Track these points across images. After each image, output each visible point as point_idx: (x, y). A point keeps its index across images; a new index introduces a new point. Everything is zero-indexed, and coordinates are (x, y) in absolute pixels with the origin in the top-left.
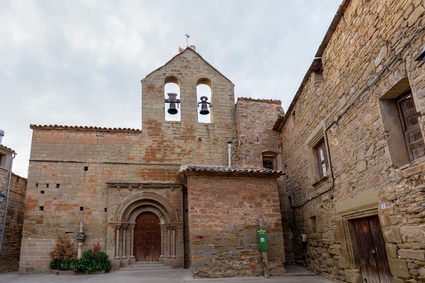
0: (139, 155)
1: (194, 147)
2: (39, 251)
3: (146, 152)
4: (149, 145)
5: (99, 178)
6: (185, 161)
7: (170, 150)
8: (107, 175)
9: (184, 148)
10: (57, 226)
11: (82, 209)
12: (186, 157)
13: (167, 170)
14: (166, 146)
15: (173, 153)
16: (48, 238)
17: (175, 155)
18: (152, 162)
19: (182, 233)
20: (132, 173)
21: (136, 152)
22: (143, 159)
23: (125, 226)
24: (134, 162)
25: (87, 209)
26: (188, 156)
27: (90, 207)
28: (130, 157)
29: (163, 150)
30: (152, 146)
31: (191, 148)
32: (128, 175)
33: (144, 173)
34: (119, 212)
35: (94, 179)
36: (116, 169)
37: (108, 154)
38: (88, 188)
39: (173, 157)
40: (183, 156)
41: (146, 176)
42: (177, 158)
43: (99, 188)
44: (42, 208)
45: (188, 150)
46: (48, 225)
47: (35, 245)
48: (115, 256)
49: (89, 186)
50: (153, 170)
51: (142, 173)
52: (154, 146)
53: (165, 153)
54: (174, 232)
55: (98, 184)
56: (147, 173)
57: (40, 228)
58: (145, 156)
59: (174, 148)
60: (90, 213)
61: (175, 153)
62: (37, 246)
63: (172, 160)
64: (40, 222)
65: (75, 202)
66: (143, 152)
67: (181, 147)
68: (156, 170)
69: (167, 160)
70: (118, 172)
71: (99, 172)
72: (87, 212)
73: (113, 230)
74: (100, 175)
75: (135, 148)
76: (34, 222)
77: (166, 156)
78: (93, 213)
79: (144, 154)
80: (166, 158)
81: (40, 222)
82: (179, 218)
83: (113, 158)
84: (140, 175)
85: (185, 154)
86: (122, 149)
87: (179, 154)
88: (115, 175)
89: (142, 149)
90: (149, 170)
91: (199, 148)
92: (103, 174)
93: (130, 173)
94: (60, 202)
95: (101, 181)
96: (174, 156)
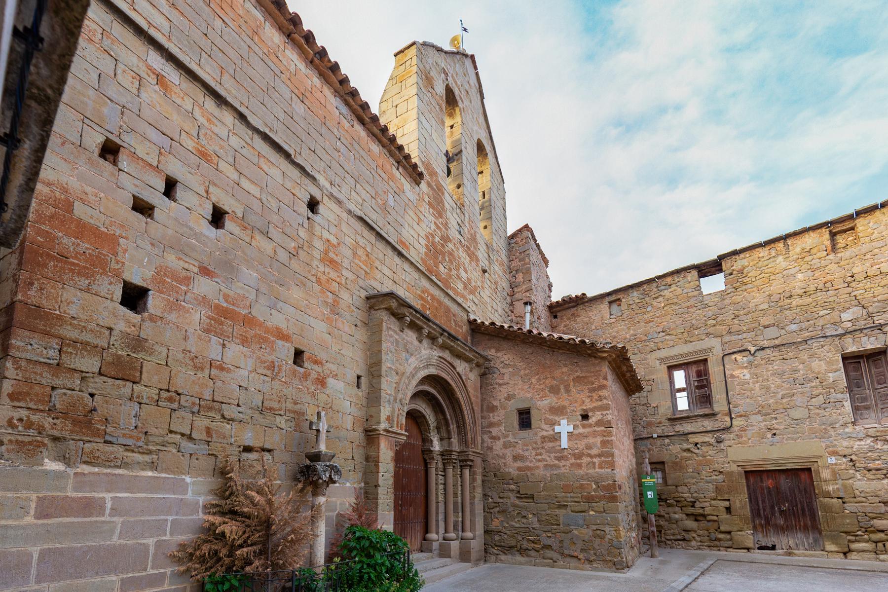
2: (115, 540)
10: (210, 409)
11: (298, 355)
16: (167, 470)
25: (317, 362)
27: (322, 356)
35: (335, 258)
38: (319, 282)
44: (134, 297)
46: (170, 400)
47: (89, 507)
49: (324, 279)
54: (467, 472)
57: (119, 406)
60: (322, 382)
62: (101, 510)
64: (124, 371)
65: (277, 320)
72: (314, 375)
76: (90, 364)
78: (331, 381)
81: (124, 371)
94: (226, 297)
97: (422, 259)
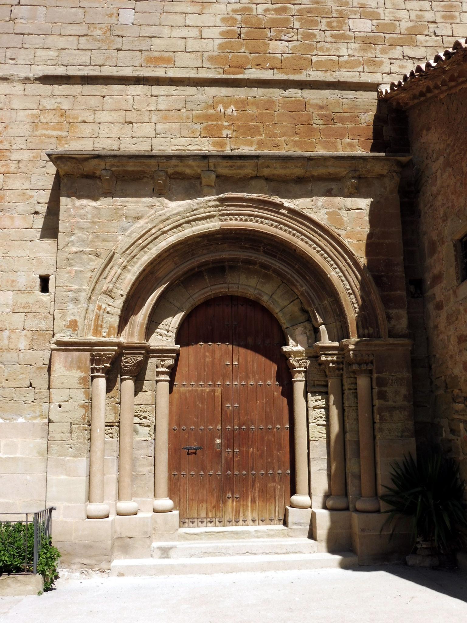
0: (192, 45)
1: (429, 16)
3: (222, 33)
4: (238, 6)
5: (19, 143)
6: (394, 68)
7: (329, 25)
8: (54, 128)
9: (386, 16)
12: (397, 52)
13: (321, 108)
14: (310, 11)
15: (338, 38)
17: (352, 45)
18: (253, 74)
19: (403, 391)
20: (165, 120)
21: (184, 32)
22: (210, 59)
23: (129, 361)
24: (172, 73)
26: (408, 51)
28: (157, 54)
29: (297, 25)
30: (250, 9)
31: (419, 17)
32: (147, 130)
33: (218, 117)
34: (108, 293)
36: (94, 102)
37: (61, 42)
39: (344, 51)
40: (383, 52)
41: (225, 133)
42: (359, 56)
43: (17, 184)
45: (404, 25)
48: (89, 499)
50: (256, 104)
51: (208, 117)
52: (260, 9)
53: (309, 36)
55: (13, 167)
56: (229, 118)
58: (220, 46)
59: (343, 17)
61: (349, 38)
63: (339, 66)
66: (215, 33)
67: (372, 15)
68: (269, 104)
69: (319, 66)
70: (104, 116)
71: (22, 115)
73: (78, 374)
74: (24, 130)
75: (179, 19)
77: (311, 48)
79: (217, 42)
80: (314, 59)
82: (389, 318)
83: (84, 58)
84: (198, 127)
85: (394, 44)
86: (122, 20)
87: (368, 42)
88: (87, 130)
89: (207, 20)
90: (242, 104)
91: (452, 17)
92: (35, 124)
93: (154, 118)
95: (26, 155)
96: (345, 50)
97: (210, 59)
